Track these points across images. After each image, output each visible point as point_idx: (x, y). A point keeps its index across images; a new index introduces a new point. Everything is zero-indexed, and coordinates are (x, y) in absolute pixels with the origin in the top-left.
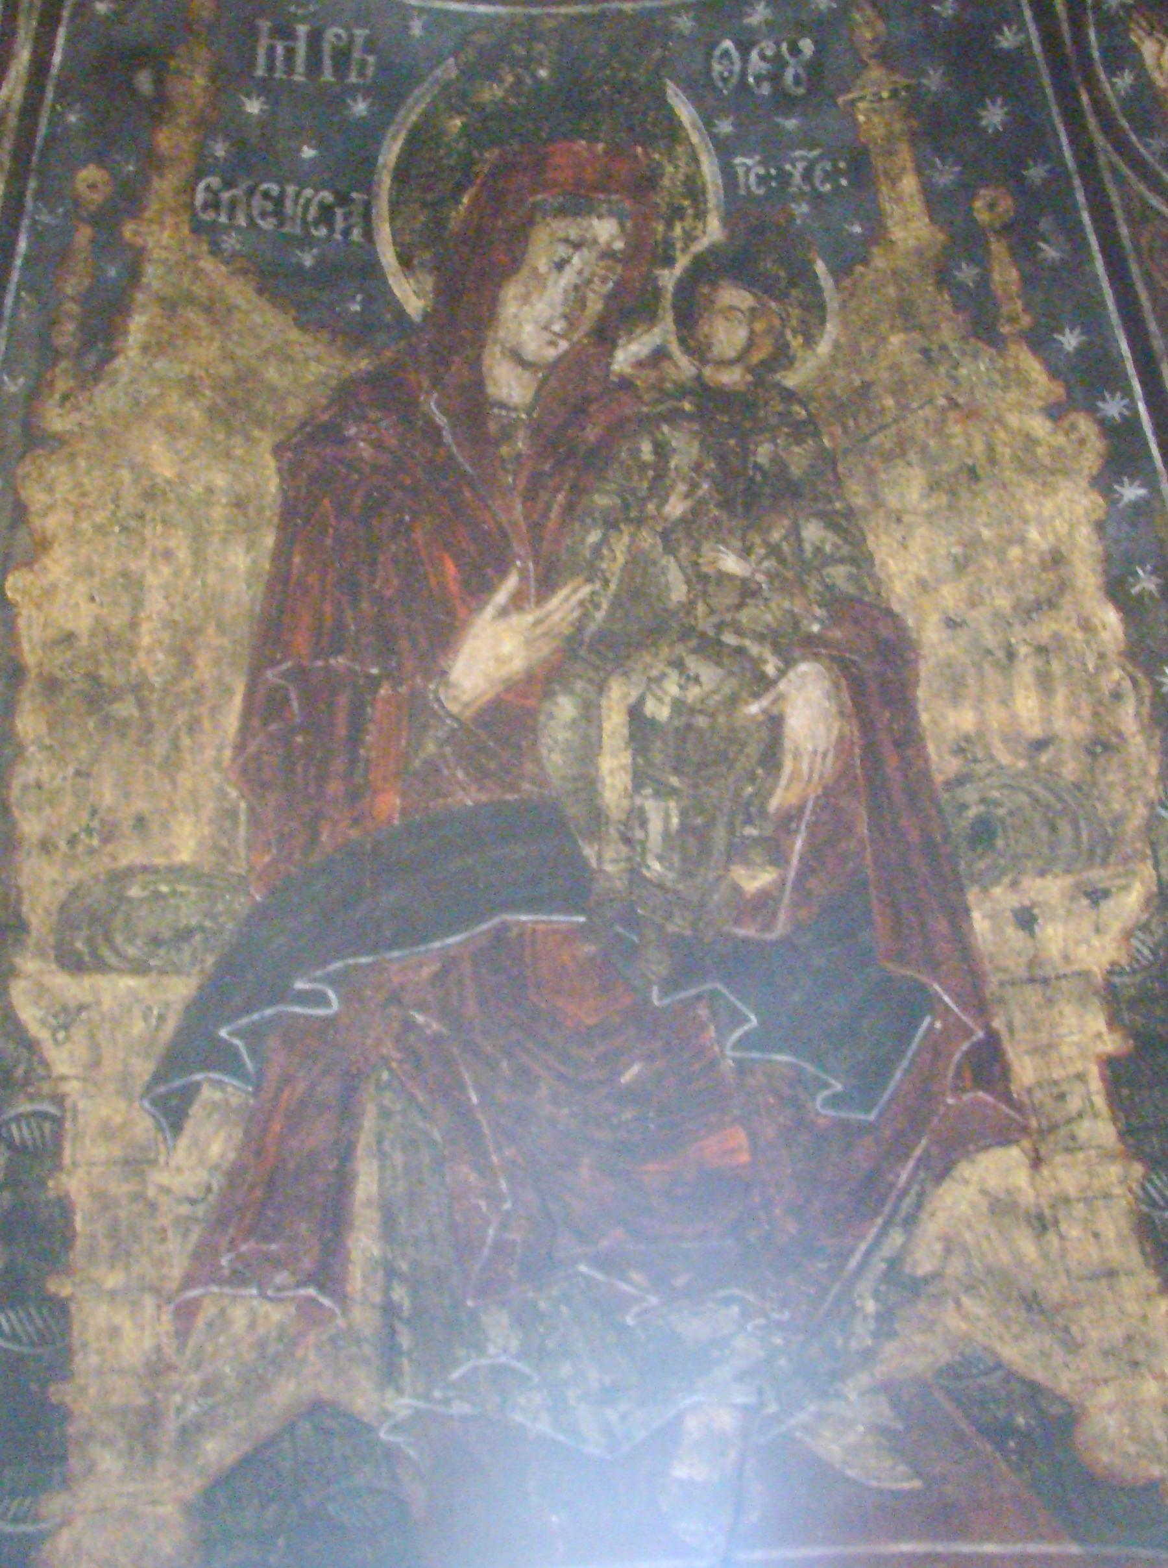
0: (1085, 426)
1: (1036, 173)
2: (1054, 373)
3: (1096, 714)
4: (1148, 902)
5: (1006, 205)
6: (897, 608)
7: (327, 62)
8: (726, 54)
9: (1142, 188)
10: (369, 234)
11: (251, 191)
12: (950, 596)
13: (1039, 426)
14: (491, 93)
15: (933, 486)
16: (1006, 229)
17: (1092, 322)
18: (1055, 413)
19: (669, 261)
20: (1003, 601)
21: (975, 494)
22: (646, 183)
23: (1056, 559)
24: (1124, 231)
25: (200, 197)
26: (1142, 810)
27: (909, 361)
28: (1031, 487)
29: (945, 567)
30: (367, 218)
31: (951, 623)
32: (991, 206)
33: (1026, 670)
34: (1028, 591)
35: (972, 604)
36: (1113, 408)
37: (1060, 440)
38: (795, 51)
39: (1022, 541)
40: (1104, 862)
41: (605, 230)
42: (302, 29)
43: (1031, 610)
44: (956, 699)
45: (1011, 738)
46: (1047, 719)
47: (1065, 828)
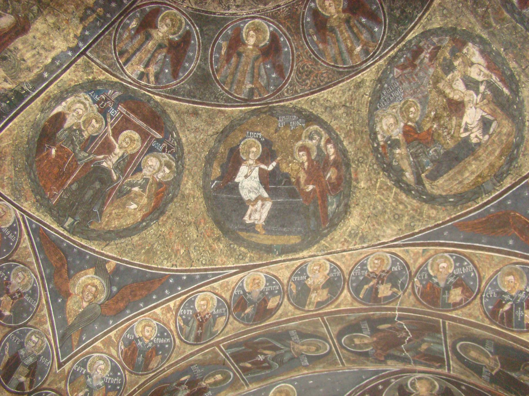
0: (76, 41)
1: (109, 15)
2: (81, 33)
3: (34, 66)
4: (10, 88)
5: (101, 14)
6: (31, 27)
9: (114, 32)
12: (38, 35)
13: (72, 35)
15: (54, 24)
16: (98, 15)
17: (91, 36)
18: (75, 36)
20: (42, 43)
21: (56, 30)
23: (54, 48)
24: (107, 33)
26: (23, 80)
27: (70, 10)
28: (62, 38)
29: (42, 31)
31: (34, 37)
32: (100, 11)
33: (34, 52)
34: (46, 46)
35: (39, 39)
36: (81, 45)
37: (72, 39)
39: (53, 41)
40: (12, 79)
43: (43, 48)
44: (23, 44)
45: (22, 55)
46: (28, 59)
47: (13, 70)
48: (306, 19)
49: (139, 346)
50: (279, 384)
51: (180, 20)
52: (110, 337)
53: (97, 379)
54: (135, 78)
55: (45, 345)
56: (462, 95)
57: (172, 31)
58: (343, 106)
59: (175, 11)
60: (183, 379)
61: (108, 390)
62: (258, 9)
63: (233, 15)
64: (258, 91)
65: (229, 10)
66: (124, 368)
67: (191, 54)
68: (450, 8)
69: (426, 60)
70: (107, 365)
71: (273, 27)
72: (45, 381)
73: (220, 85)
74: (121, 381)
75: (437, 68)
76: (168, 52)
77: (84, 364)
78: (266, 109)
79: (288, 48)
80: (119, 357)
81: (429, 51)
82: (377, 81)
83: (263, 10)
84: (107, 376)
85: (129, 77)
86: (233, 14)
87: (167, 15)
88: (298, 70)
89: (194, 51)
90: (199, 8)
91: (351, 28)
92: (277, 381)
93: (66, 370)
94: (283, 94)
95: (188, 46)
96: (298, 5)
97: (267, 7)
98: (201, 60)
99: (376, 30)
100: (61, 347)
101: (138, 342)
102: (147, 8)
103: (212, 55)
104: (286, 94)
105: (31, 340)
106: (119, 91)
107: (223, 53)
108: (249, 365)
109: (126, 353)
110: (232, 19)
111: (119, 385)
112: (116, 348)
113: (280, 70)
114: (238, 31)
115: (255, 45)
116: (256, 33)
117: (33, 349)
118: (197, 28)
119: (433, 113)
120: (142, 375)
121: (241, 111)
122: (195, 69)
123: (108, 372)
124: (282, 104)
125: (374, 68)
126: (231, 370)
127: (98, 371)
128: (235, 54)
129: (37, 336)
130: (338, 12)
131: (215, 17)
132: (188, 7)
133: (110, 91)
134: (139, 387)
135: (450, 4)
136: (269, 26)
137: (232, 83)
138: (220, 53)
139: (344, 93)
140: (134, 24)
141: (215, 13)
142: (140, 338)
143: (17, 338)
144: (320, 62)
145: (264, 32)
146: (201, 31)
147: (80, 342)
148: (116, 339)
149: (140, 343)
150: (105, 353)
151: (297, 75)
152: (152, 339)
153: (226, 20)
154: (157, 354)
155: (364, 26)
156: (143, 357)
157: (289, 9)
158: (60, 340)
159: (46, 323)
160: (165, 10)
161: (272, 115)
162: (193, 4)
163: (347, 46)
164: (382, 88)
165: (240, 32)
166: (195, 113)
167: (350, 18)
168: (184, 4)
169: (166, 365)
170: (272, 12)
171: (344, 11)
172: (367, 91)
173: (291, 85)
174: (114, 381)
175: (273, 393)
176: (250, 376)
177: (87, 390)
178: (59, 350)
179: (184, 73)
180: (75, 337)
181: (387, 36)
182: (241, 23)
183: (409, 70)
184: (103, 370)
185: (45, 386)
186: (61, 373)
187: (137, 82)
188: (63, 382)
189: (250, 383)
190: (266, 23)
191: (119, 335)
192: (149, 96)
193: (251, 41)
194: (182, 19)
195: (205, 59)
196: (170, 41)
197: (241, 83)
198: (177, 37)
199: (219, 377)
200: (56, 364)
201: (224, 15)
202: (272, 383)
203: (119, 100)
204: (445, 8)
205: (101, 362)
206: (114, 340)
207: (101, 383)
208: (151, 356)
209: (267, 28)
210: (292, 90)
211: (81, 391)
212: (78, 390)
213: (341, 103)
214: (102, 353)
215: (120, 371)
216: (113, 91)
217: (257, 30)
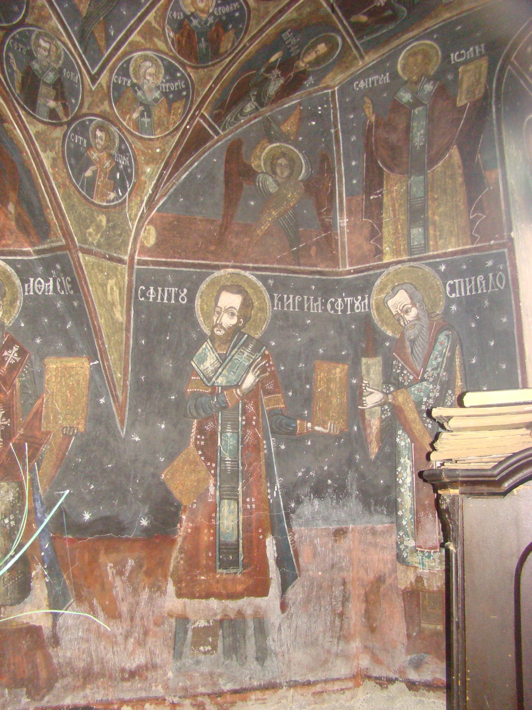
49: (196, 27)
50: (409, 44)
52: (149, 23)
53: (151, 90)
55: (62, 53)
60: (273, 59)
61: (170, 103)
66: (183, 65)
70: (158, 66)
72: (82, 104)
74: (185, 84)
77: (124, 72)
80: (171, 50)
84: (162, 82)
92: (405, 42)
93: (104, 85)
100: (85, 52)
101: (191, 21)
105: (40, 46)
108: (364, 19)
109: (179, 42)
111: (183, 90)
112: (162, 38)
117: (48, 60)
120: (213, 65)
123: (161, 76)
126: (339, 32)
127: (148, 78)
129: (46, 39)
134: (216, 83)
142: (192, 14)
143: (21, 46)
147: (109, 39)
148: (159, 23)
149: (195, 22)
150: (149, 49)
152: (211, 11)
154: (226, 30)
156: (206, 41)
158: (80, 43)
159: (50, 18)
169: (246, 40)
174: (174, 86)
175: (403, 58)
176: (366, 39)
177: (141, 108)
178: (83, 56)
180: (99, 35)
184: (155, 75)
185: (85, 110)
186: (98, 91)
188: (106, 103)
189: (367, 53)
191: (160, 17)
199: (322, 48)
200: (88, 79)
202: (398, 46)
205: (148, 64)
206: (157, 26)
207: (157, 94)
208: (218, 36)
211: (134, 111)
212: (130, 110)
214: (145, 50)
215: (179, 71)
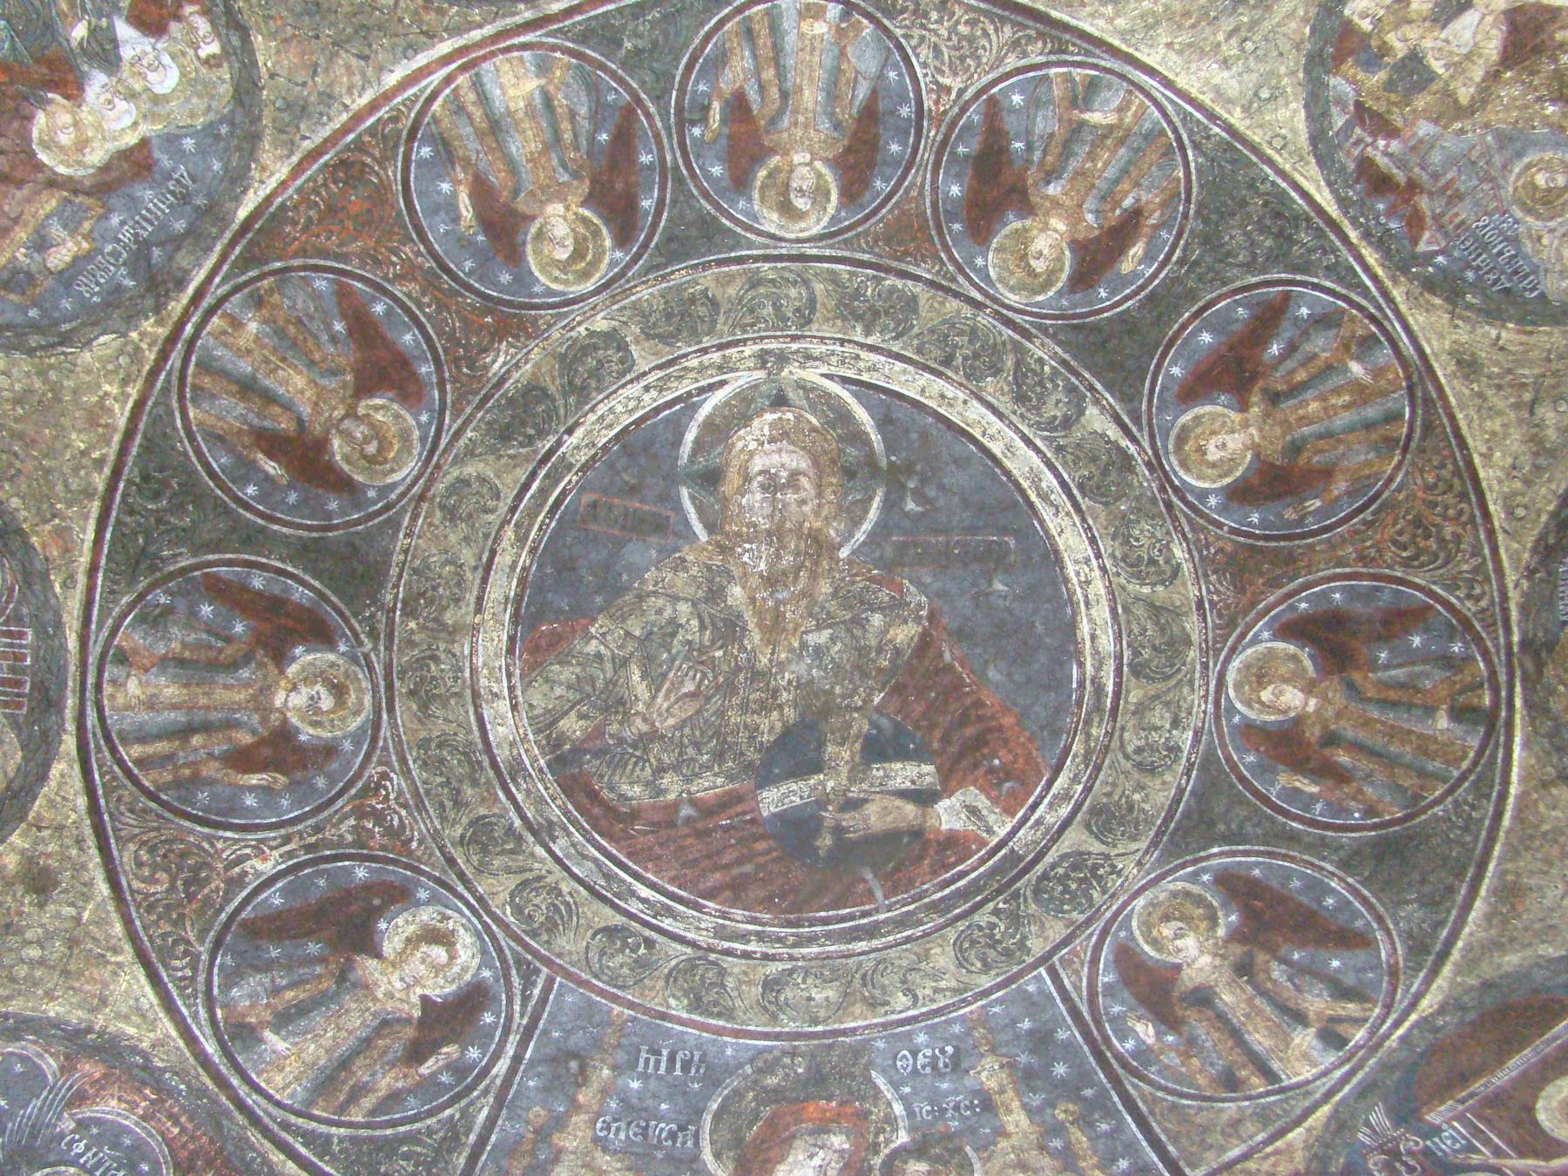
1: (1088, 1092)
7: (678, 1066)
8: (904, 1057)
10: (697, 1143)
11: (629, 1124)
14: (772, 1081)
19: (877, 1153)
22: (864, 1115)
25: (599, 1125)
30: (696, 1136)
38: (943, 1051)
41: (838, 1141)
42: (665, 1052)
48: (1250, 525)
51: (1174, 894)
54: (1331, 1057)
56: (1489, 19)
57: (1204, 925)
58: (1532, 413)
59: (1140, 902)
62: (1198, 667)
63: (1199, 742)
64: (1461, 692)
65: (1179, 749)
67: (1296, 883)
68: (1254, 76)
69: (1395, 146)
71: (1261, 631)
73: (1424, 811)
75: (1414, 111)
76: (1273, 952)
78: (1529, 665)
79: (1333, 590)
81: (1369, 140)
82: (1455, 305)
83: (1205, 653)
85: (1325, 1074)
86: (1197, 735)
87: (1147, 926)
88: (1406, 563)
89: (1288, 875)
90: (1152, 834)
91: (1295, 390)
94: (1483, 611)
95: (1268, 889)
96: (1207, 547)
97: (1195, 637)
98: (1324, 859)
99: (1304, 311)
102: (1106, 978)
103: (1313, 823)
104: (1484, 603)
106: (1370, 1109)
107: (1314, 789)
110: (1210, 743)
113: (1399, 620)
114: (1250, 732)
115: (1309, 689)
116: (1270, 683)
118: (1215, 850)
119: (1550, 109)
121: (1526, 745)
122: (1350, 880)
124: (1514, 615)
125: (1417, 320)
128: (1327, 752)
130: (1245, 425)
131: (1193, 793)
132: (1139, 864)
133: (1360, 1136)
135: (1245, 76)
136: (1256, 640)
137: (1422, 773)
138: (1314, 798)
139: (1493, 412)
140: (1146, 1031)
141: (1181, 791)
144: (1386, 494)
145: (1270, 655)
146: (1226, 839)
151: (1422, 565)
153: (1209, 762)
155: (1292, 348)
157: (1215, 572)
160: (1129, 929)
161: (1550, 646)
162: (1134, 846)
163: (1346, 407)
164: (1478, 286)
165: (1257, 727)
166: (1510, 893)
167: (1264, 391)
168: (1125, 873)
170: (1216, 627)
171: (1243, 407)
172: (1484, 336)
173: (1452, 587)
179: (1356, 914)
181: (1327, 277)
182: (1229, 720)
183: (1424, 203)
187: (1353, 1054)
190: (1244, 649)
192: (1413, 1026)
193: (1292, 698)
194: (1171, 887)
195: (1320, 847)
196: (1235, 936)
197: (1425, 746)
198: (1227, 915)
201: (1192, 765)
203: (1406, 1113)
204: (1256, 94)
209: (1260, 648)
210: (1471, 583)
213: (1520, 421)
216: (1365, 1129)
217: (1260, 675)
